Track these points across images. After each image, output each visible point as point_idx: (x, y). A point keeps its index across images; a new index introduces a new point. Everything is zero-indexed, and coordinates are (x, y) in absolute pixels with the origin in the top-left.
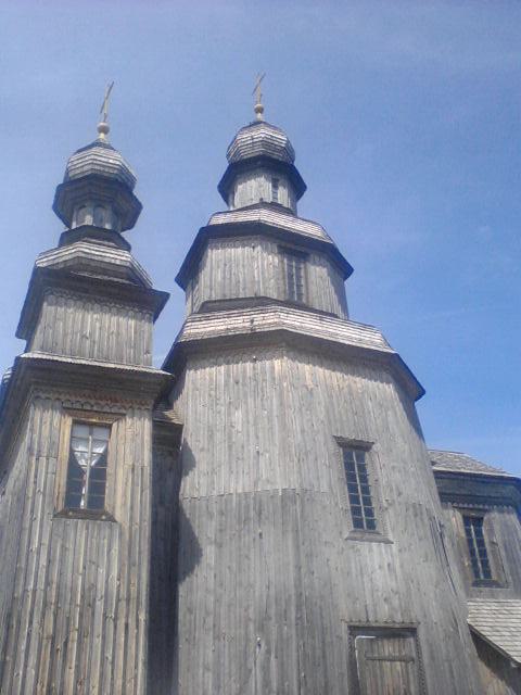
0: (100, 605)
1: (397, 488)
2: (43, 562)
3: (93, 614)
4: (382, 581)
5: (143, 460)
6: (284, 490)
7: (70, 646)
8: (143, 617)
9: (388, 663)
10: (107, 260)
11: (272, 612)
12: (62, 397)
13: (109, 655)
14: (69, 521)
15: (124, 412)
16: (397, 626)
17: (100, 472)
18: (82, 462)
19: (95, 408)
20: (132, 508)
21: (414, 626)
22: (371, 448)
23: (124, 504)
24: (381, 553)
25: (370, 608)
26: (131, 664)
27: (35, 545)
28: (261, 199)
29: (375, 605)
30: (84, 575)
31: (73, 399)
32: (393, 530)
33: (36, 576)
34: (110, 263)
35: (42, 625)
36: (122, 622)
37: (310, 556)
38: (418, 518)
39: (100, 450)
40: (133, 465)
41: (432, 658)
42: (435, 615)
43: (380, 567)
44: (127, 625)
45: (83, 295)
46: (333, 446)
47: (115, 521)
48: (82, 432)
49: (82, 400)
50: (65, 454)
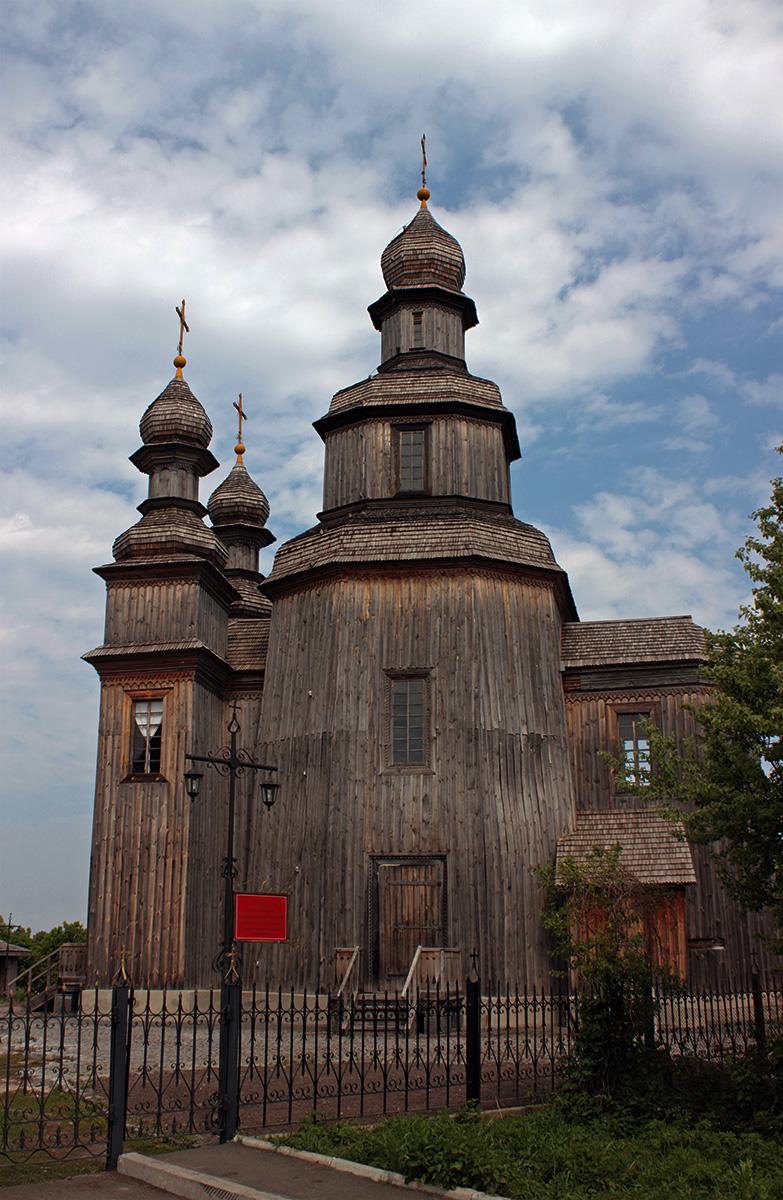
0: (153, 847)
1: (451, 715)
2: (113, 818)
3: (149, 855)
4: (413, 811)
5: (187, 727)
6: (324, 733)
7: (134, 877)
8: (185, 856)
9: (411, 888)
10: (154, 540)
11: (307, 845)
12: (123, 683)
13: (161, 884)
14: (131, 785)
15: (172, 686)
16: (423, 854)
17: (156, 742)
18: (144, 733)
19: (148, 687)
20: (177, 770)
21: (444, 853)
22: (429, 674)
23: (172, 767)
24: (418, 786)
25: (394, 839)
26: (177, 891)
27: (107, 807)
28: (398, 349)
29: (401, 836)
30: (141, 826)
31: (131, 682)
32: (438, 761)
33: (109, 829)
34: (157, 543)
35: (114, 864)
36: (169, 861)
37: (338, 795)
38: (471, 744)
39: (156, 720)
40: (179, 732)
41: (458, 883)
42: (467, 842)
43: (414, 799)
44: (174, 862)
45: (136, 581)
46: (380, 680)
47: (165, 781)
48: (142, 708)
49: (138, 682)
50: (126, 729)
